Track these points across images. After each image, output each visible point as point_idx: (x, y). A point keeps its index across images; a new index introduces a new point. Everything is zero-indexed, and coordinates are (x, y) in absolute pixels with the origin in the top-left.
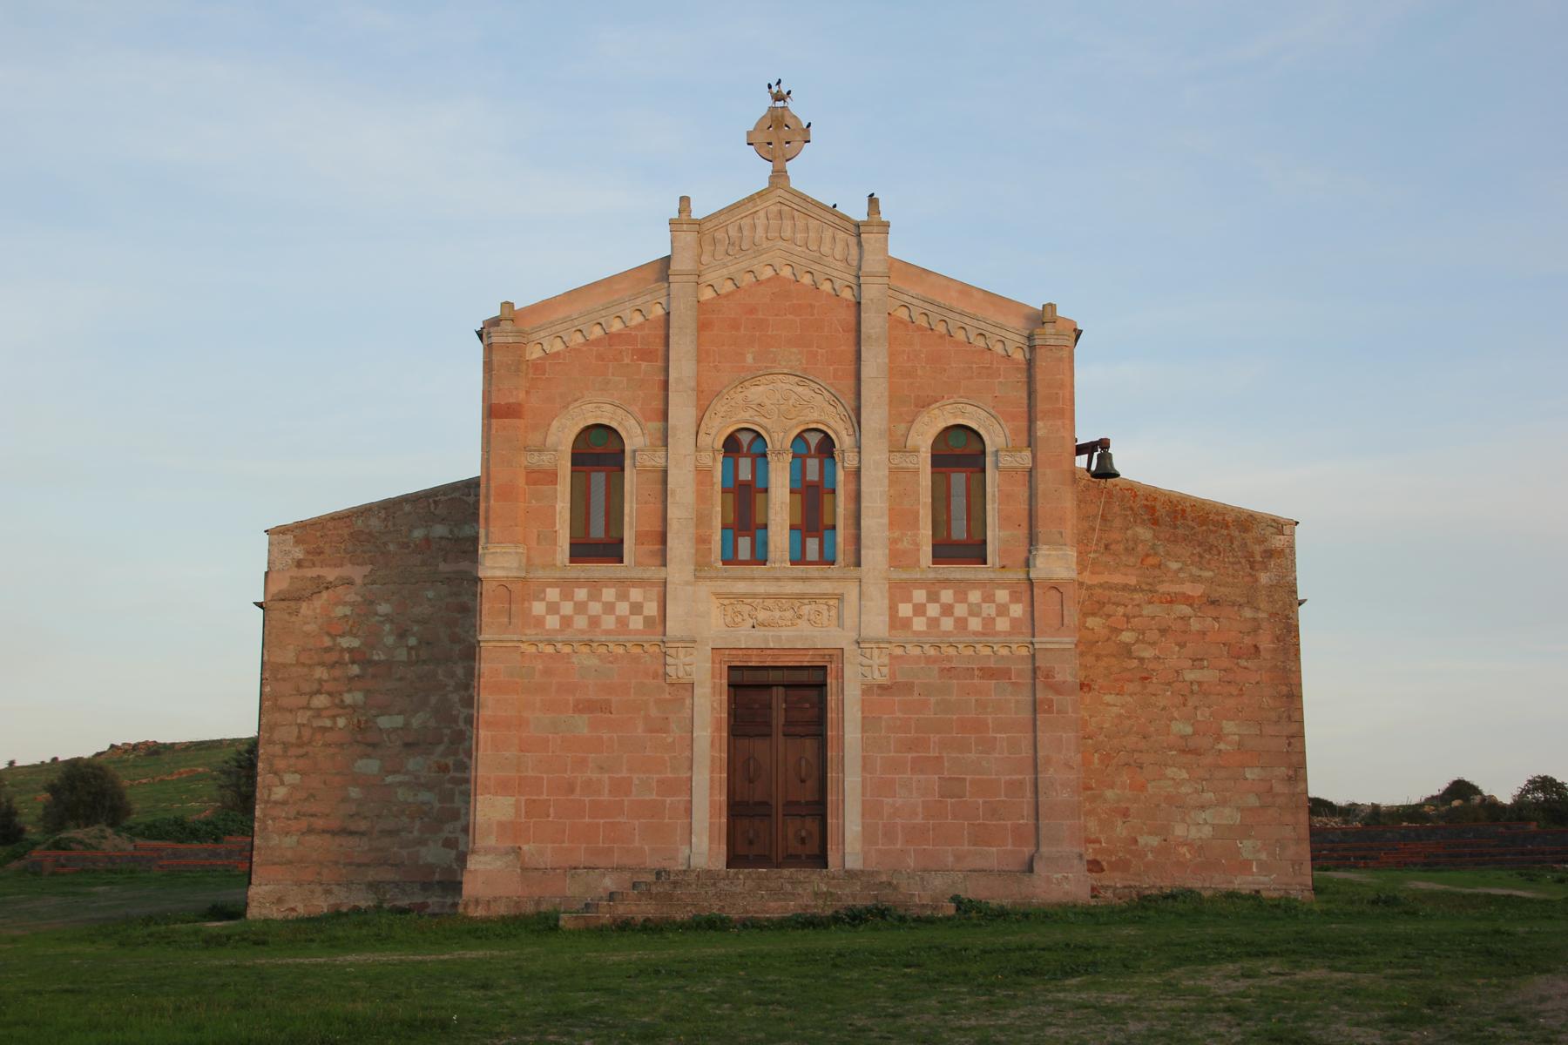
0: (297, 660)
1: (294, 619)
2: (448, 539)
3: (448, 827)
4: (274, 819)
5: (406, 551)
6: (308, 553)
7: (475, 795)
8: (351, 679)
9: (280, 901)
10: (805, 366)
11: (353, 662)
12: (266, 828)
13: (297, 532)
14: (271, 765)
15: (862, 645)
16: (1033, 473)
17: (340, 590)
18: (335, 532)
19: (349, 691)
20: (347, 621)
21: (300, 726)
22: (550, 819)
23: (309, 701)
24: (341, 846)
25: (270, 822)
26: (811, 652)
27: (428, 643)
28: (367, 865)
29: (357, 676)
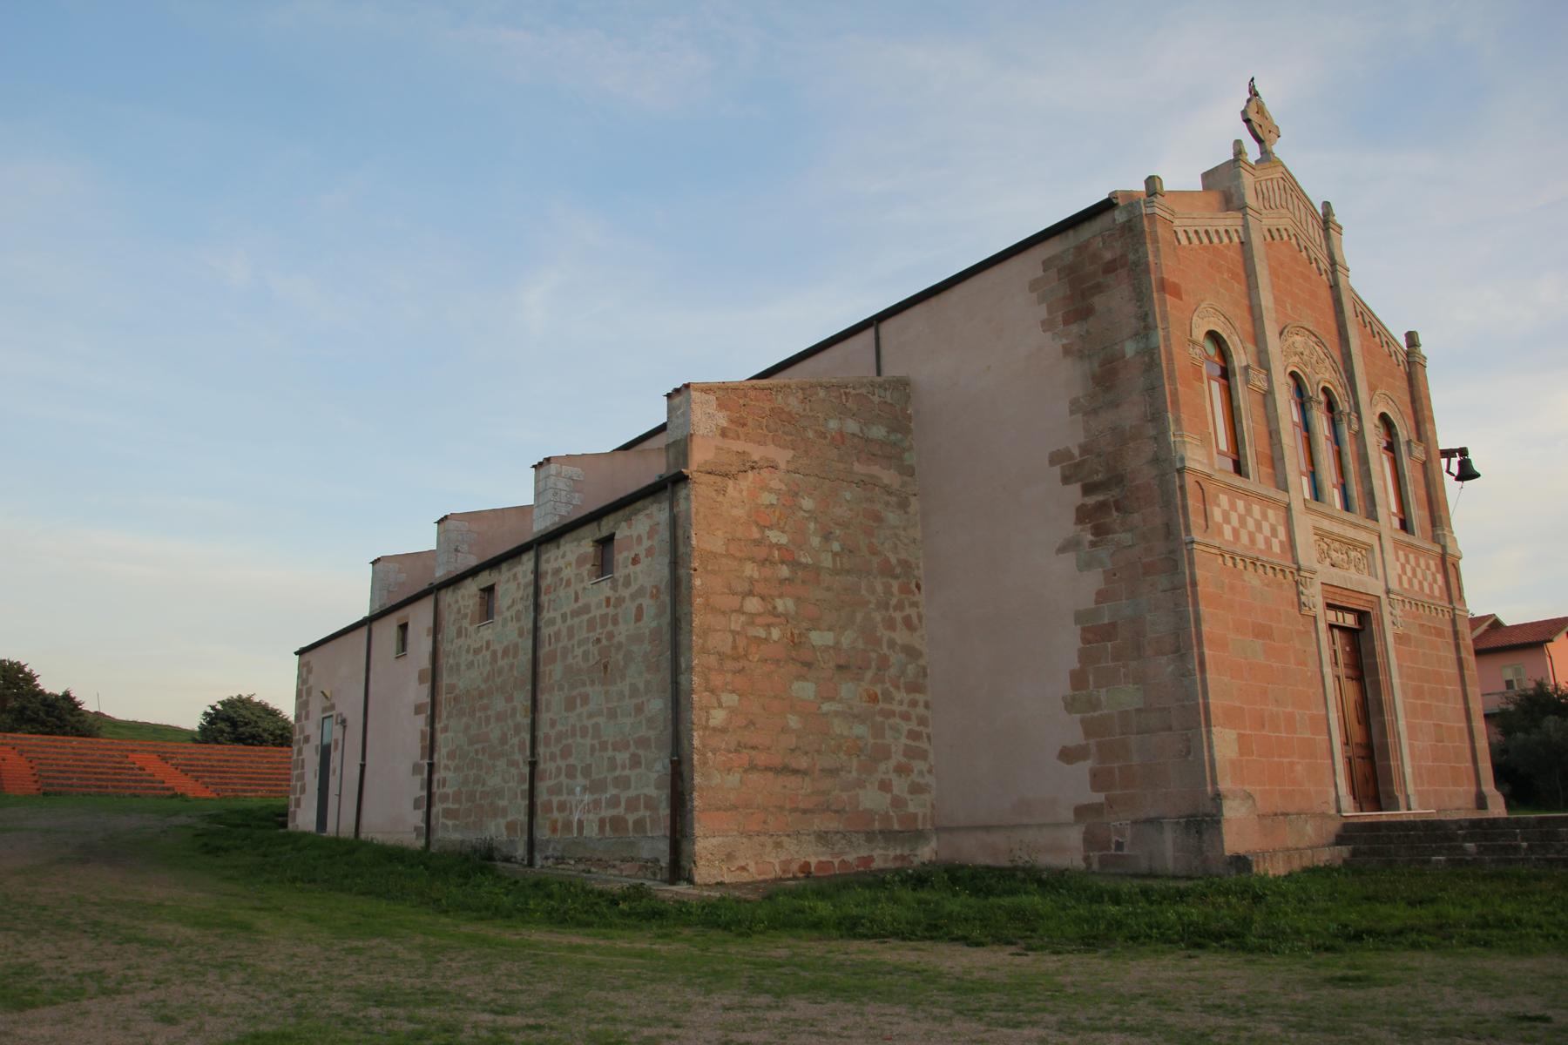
0: (727, 550)
1: (720, 498)
2: (859, 437)
3: (882, 767)
4: (714, 751)
5: (824, 442)
6: (732, 421)
7: (1208, 725)
8: (782, 581)
9: (730, 857)
11: (783, 562)
12: (705, 763)
13: (720, 393)
14: (707, 680)
15: (1391, 596)
16: (1429, 465)
17: (765, 473)
18: (757, 404)
19: (781, 596)
20: (774, 512)
21: (735, 633)
22: (1254, 757)
23: (742, 603)
24: (785, 787)
25: (710, 754)
26: (1364, 597)
27: (850, 551)
28: (811, 811)
29: (786, 579)
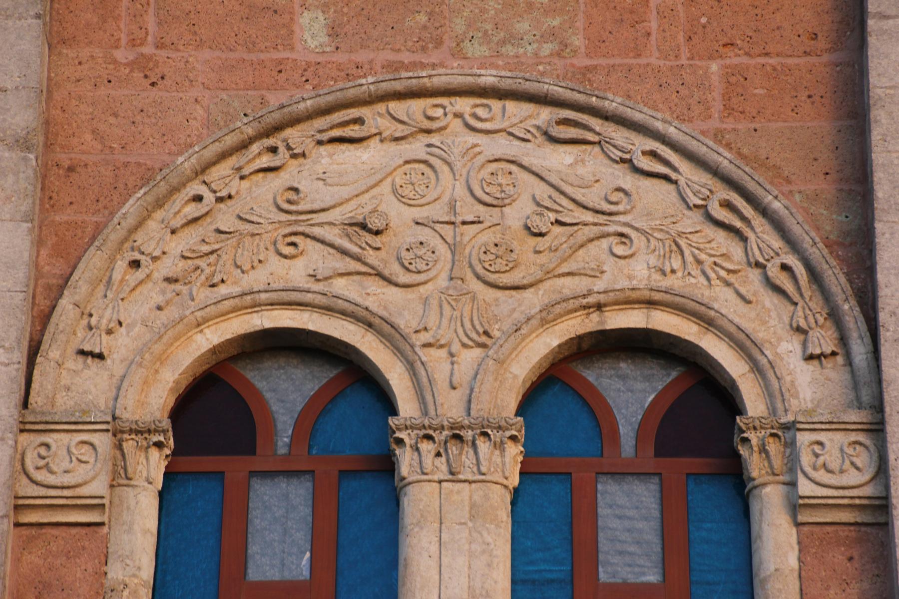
10: (582, 61)
